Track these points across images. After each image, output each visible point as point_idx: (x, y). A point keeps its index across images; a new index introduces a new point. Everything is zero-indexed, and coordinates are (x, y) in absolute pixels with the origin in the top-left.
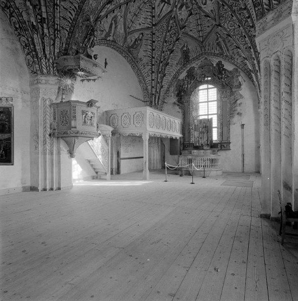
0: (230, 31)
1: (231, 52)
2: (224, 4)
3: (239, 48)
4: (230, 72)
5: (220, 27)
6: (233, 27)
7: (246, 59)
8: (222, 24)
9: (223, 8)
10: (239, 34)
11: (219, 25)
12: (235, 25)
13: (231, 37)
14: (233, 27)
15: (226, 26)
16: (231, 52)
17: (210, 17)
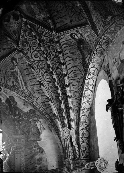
0: (33, 62)
1: (30, 88)
2: (32, 29)
3: (42, 85)
4: (25, 114)
5: (22, 54)
6: (38, 59)
7: (50, 100)
8: (25, 52)
9: (29, 33)
10: (45, 69)
11: (22, 51)
12: (41, 57)
13: (34, 70)
14: (38, 59)
15: (29, 54)
16: (30, 88)
17: (10, 38)
